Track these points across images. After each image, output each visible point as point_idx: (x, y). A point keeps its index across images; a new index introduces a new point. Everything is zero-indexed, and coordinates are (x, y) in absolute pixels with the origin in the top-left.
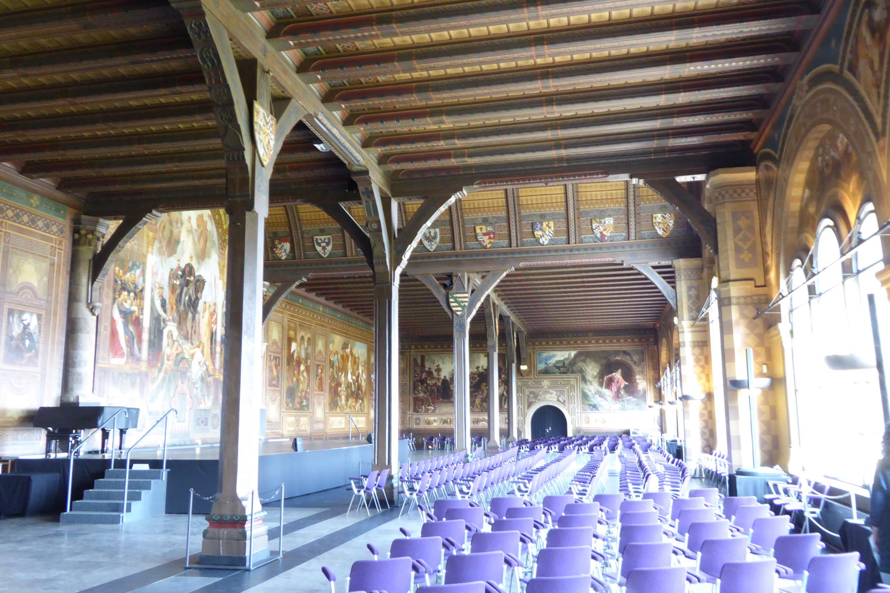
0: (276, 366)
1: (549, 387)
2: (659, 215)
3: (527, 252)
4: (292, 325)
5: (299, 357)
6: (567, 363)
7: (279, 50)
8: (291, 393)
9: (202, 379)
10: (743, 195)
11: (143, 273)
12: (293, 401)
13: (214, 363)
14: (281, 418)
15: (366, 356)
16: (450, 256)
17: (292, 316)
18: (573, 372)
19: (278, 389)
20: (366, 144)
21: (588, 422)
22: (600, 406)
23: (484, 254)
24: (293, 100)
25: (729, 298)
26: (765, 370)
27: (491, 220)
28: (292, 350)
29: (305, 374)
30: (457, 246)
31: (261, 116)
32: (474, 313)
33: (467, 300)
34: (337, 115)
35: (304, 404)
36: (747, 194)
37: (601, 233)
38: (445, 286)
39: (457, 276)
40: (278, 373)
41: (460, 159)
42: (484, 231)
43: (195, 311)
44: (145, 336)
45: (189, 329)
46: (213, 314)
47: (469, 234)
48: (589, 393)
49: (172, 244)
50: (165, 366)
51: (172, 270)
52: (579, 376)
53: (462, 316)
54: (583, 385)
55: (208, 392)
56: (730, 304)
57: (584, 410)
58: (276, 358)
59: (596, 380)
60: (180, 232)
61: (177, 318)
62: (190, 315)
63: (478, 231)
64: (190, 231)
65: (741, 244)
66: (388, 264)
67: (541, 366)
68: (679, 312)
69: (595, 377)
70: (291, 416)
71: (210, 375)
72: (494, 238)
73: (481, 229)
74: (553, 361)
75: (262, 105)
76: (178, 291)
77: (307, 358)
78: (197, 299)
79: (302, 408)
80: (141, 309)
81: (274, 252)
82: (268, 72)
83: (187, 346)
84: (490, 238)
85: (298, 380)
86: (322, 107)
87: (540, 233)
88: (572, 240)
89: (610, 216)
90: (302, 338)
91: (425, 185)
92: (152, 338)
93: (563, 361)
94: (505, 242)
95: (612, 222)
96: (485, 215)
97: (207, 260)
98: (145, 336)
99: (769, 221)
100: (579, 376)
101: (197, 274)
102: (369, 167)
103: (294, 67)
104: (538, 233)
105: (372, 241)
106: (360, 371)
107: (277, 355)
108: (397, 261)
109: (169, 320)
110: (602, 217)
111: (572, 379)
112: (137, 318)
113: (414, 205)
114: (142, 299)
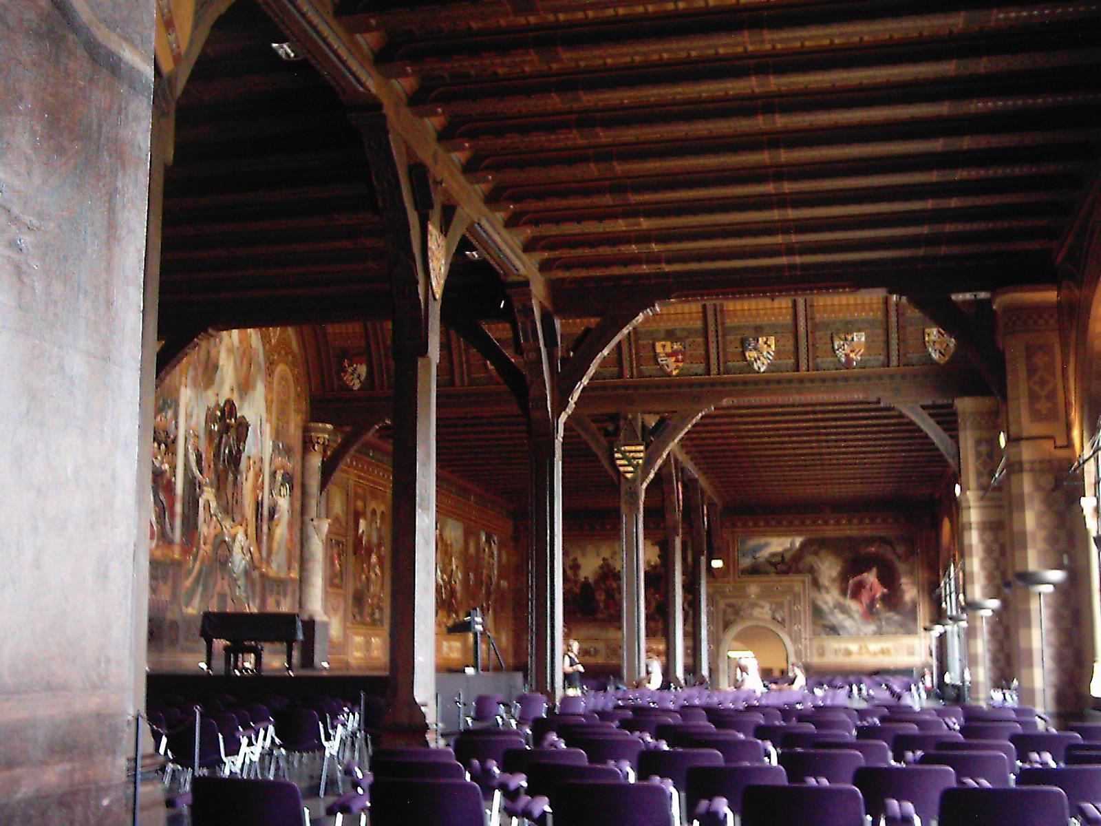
0: (339, 556)
1: (759, 597)
2: (935, 331)
3: (734, 383)
4: (360, 491)
5: (369, 541)
6: (788, 556)
7: (449, 151)
9: (247, 573)
10: (1041, 322)
11: (176, 417)
13: (260, 550)
14: (346, 636)
15: (462, 541)
16: (615, 387)
17: (360, 477)
18: (798, 572)
19: (342, 591)
20: (528, 247)
21: (822, 654)
22: (843, 627)
23: (669, 386)
24: (459, 209)
25: (1021, 463)
26: (1066, 561)
27: (679, 334)
28: (360, 531)
30: (627, 374)
31: (434, 237)
32: (652, 476)
33: (642, 455)
34: (500, 216)
35: (377, 616)
36: (1047, 322)
37: (847, 355)
38: (607, 434)
39: (626, 418)
41: (655, 266)
42: (668, 350)
43: (237, 471)
44: (178, 508)
45: (230, 497)
46: (259, 472)
47: (646, 354)
48: (825, 608)
49: (210, 371)
50: (201, 552)
51: (209, 409)
52: (808, 578)
53: (634, 480)
54: (814, 594)
55: (253, 592)
56: (1021, 471)
57: (815, 634)
58: (338, 543)
59: (837, 585)
60: (219, 352)
61: (215, 482)
62: (231, 477)
63: (659, 349)
64: (230, 351)
65: (1037, 388)
66: (549, 409)
67: (746, 562)
68: (963, 478)
69: (833, 580)
70: (358, 634)
71: (255, 568)
72: (683, 361)
73: (664, 346)
74: (765, 554)
75: (433, 224)
76: (216, 441)
78: (240, 452)
80: (173, 468)
81: (341, 379)
82: (441, 183)
83: (227, 523)
84: (677, 361)
85: (368, 578)
86: (485, 210)
87: (754, 354)
88: (803, 366)
89: (859, 330)
90: (374, 512)
91: (604, 299)
92: (187, 509)
93: (782, 555)
94: (701, 368)
95: (863, 339)
96: (670, 326)
97: (251, 392)
98: (178, 508)
99: (1072, 360)
100: (808, 578)
101: (239, 415)
102: (530, 277)
103: (460, 166)
104: (751, 355)
105: (529, 378)
106: (454, 567)
107: (340, 539)
108: (561, 405)
109: (206, 485)
110: (850, 332)
111: (798, 583)
112: (169, 482)
113: (579, 325)
114: (174, 453)
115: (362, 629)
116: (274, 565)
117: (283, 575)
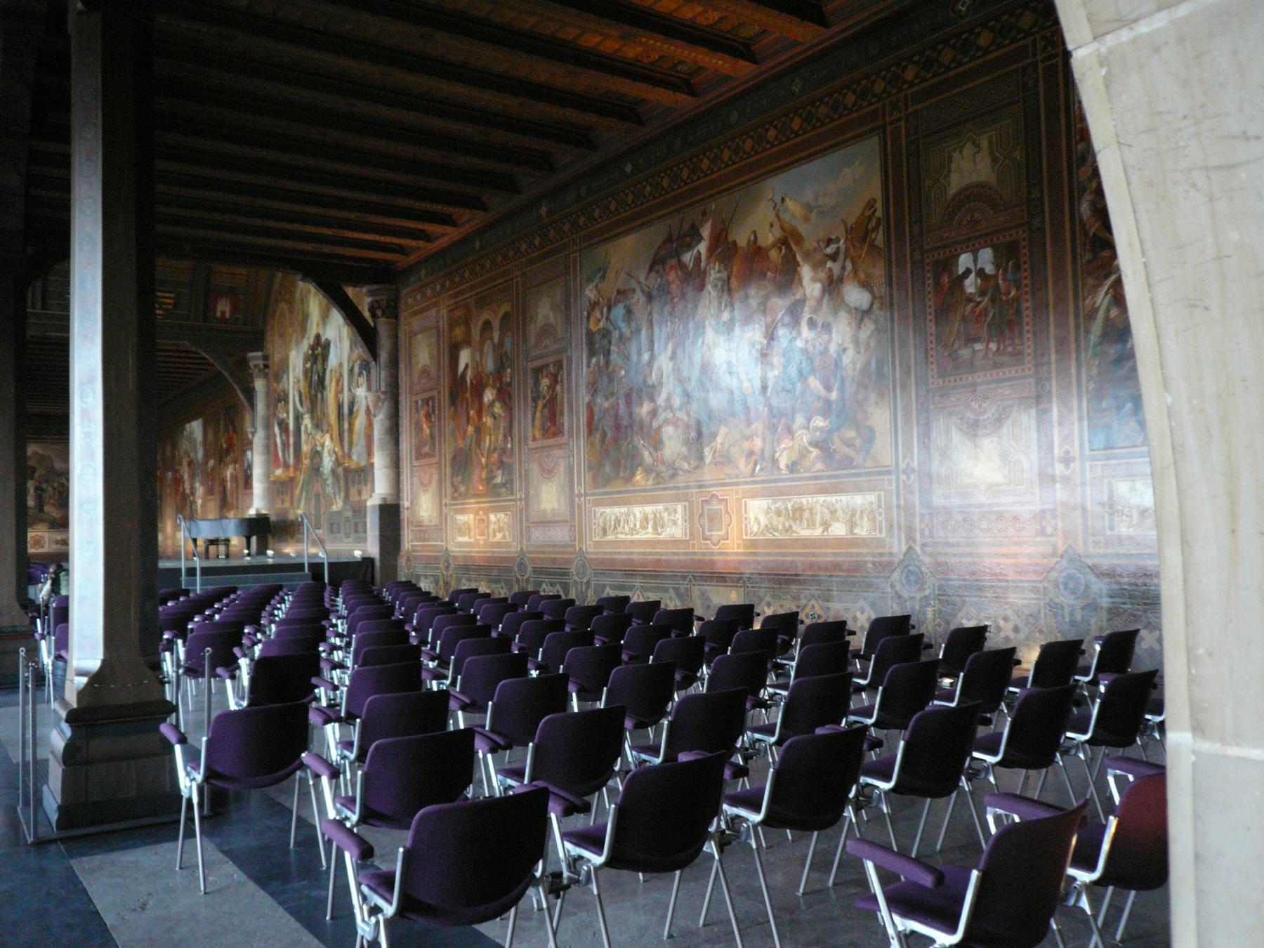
0: (428, 416)
13: (342, 447)
14: (443, 517)
19: (435, 460)
28: (461, 367)
29: (498, 409)
35: (499, 480)
58: (426, 402)
77: (500, 369)
78: (324, 370)
107: (426, 395)
116: (355, 457)
117: (363, 464)
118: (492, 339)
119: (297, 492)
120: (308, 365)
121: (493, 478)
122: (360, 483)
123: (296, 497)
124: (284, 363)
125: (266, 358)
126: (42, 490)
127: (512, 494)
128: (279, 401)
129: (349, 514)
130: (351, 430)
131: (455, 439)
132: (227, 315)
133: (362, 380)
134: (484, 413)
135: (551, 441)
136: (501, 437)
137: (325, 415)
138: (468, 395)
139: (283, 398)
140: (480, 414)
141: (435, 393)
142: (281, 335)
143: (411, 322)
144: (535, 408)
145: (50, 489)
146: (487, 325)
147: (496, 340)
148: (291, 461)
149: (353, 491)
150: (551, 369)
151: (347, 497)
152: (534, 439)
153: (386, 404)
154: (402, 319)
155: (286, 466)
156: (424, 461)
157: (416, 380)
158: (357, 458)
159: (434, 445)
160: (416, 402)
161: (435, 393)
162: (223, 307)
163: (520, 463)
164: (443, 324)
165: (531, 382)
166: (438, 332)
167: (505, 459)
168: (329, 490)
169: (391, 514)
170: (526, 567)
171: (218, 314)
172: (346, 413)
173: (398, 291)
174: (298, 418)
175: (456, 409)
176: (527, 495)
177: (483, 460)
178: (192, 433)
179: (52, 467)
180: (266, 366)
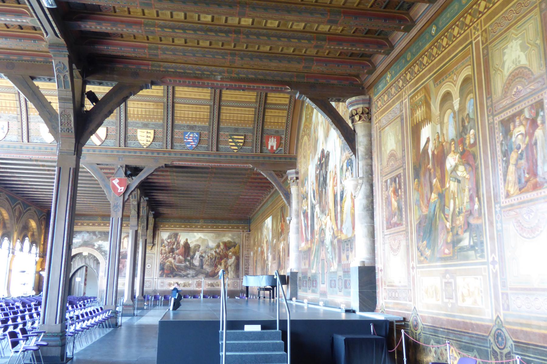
0: (396, 192)
8: (428, 228)
12: (432, 244)
13: (337, 224)
29: (461, 172)
35: (465, 243)
40: (399, 202)
55: (335, 254)
71: (336, 237)
77: (463, 131)
79: (456, 249)
115: (438, 267)
116: (344, 231)
117: (349, 235)
118: (452, 107)
119: (312, 258)
120: (318, 172)
121: (460, 241)
122: (348, 250)
123: (311, 261)
124: (306, 174)
125: (297, 173)
126: (202, 257)
127: (482, 256)
128: (304, 199)
129: (341, 273)
130: (342, 212)
131: (420, 207)
132: (275, 148)
133: (348, 174)
134: (447, 179)
135: (533, 195)
136: (466, 199)
137: (327, 203)
138: (430, 166)
139: (305, 197)
140: (442, 181)
141: (401, 171)
142: (305, 157)
143: (379, 118)
144: (507, 162)
145: (206, 256)
146: (447, 96)
147: (456, 107)
148: (309, 237)
149: (344, 256)
150: (527, 114)
151: (340, 261)
152: (508, 195)
153: (363, 187)
154: (374, 118)
155: (307, 240)
156: (393, 230)
157: (385, 163)
158: (346, 234)
159: (401, 215)
160: (386, 182)
161: (401, 171)
162: (272, 143)
163: (491, 223)
164: (407, 111)
165: (499, 136)
166: (402, 120)
167: (472, 221)
168: (329, 256)
169: (368, 276)
170: (505, 339)
171: (269, 148)
172: (339, 199)
173: (370, 101)
174: (313, 207)
175: (419, 181)
176: (502, 258)
177: (448, 225)
178: (267, 225)
179: (208, 245)
180: (297, 178)
